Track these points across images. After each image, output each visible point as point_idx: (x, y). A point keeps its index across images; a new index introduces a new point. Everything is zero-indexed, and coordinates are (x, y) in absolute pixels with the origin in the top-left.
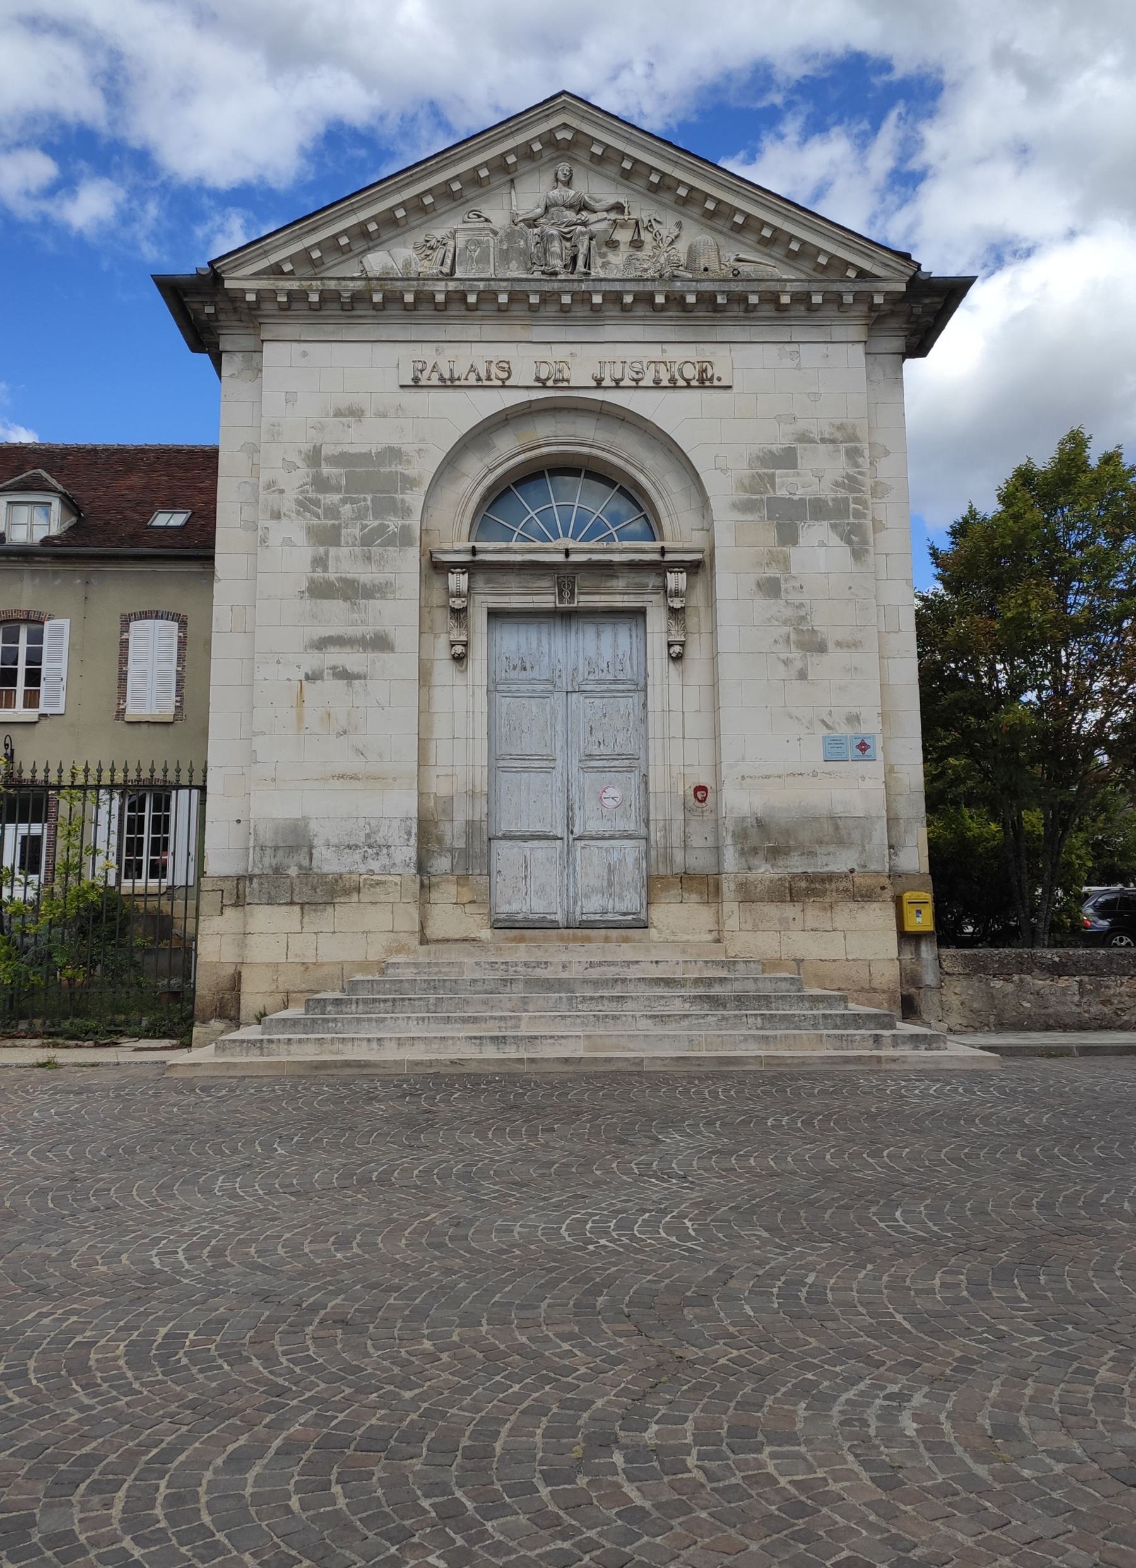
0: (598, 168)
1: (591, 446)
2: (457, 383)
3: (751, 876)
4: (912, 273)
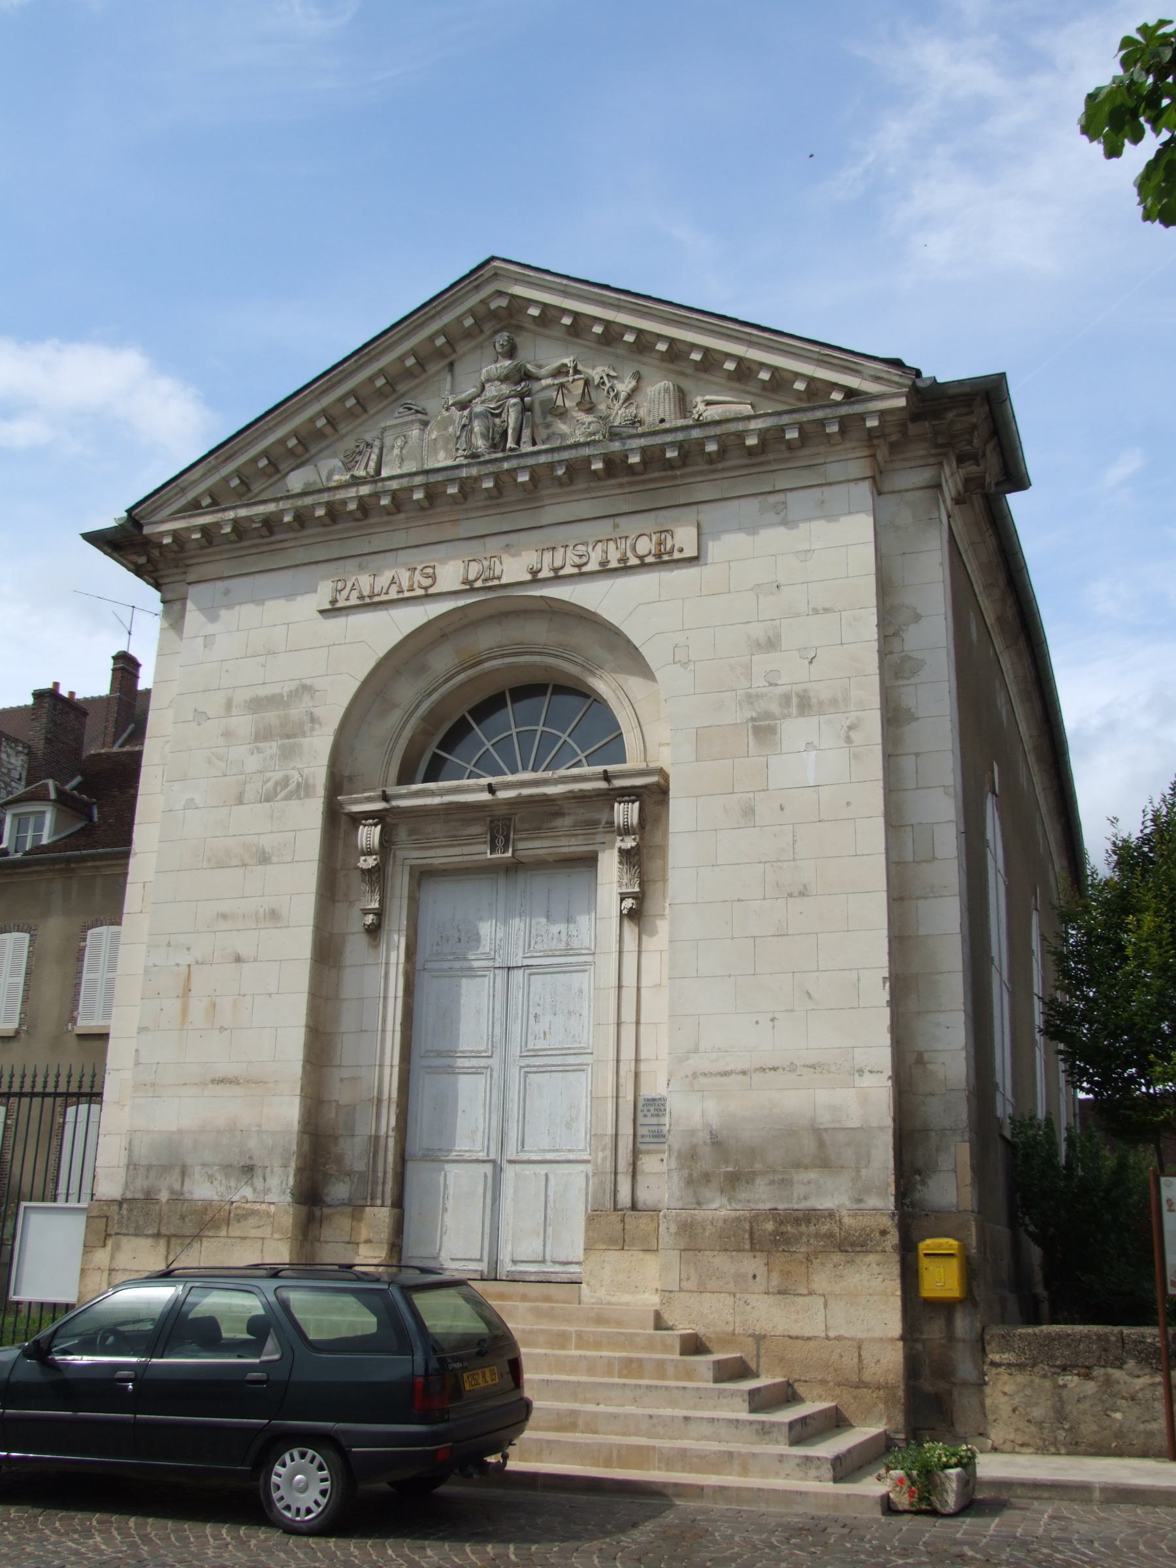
0: (547, 332)
1: (540, 654)
2: (377, 599)
3: (699, 1214)
4: (909, 383)
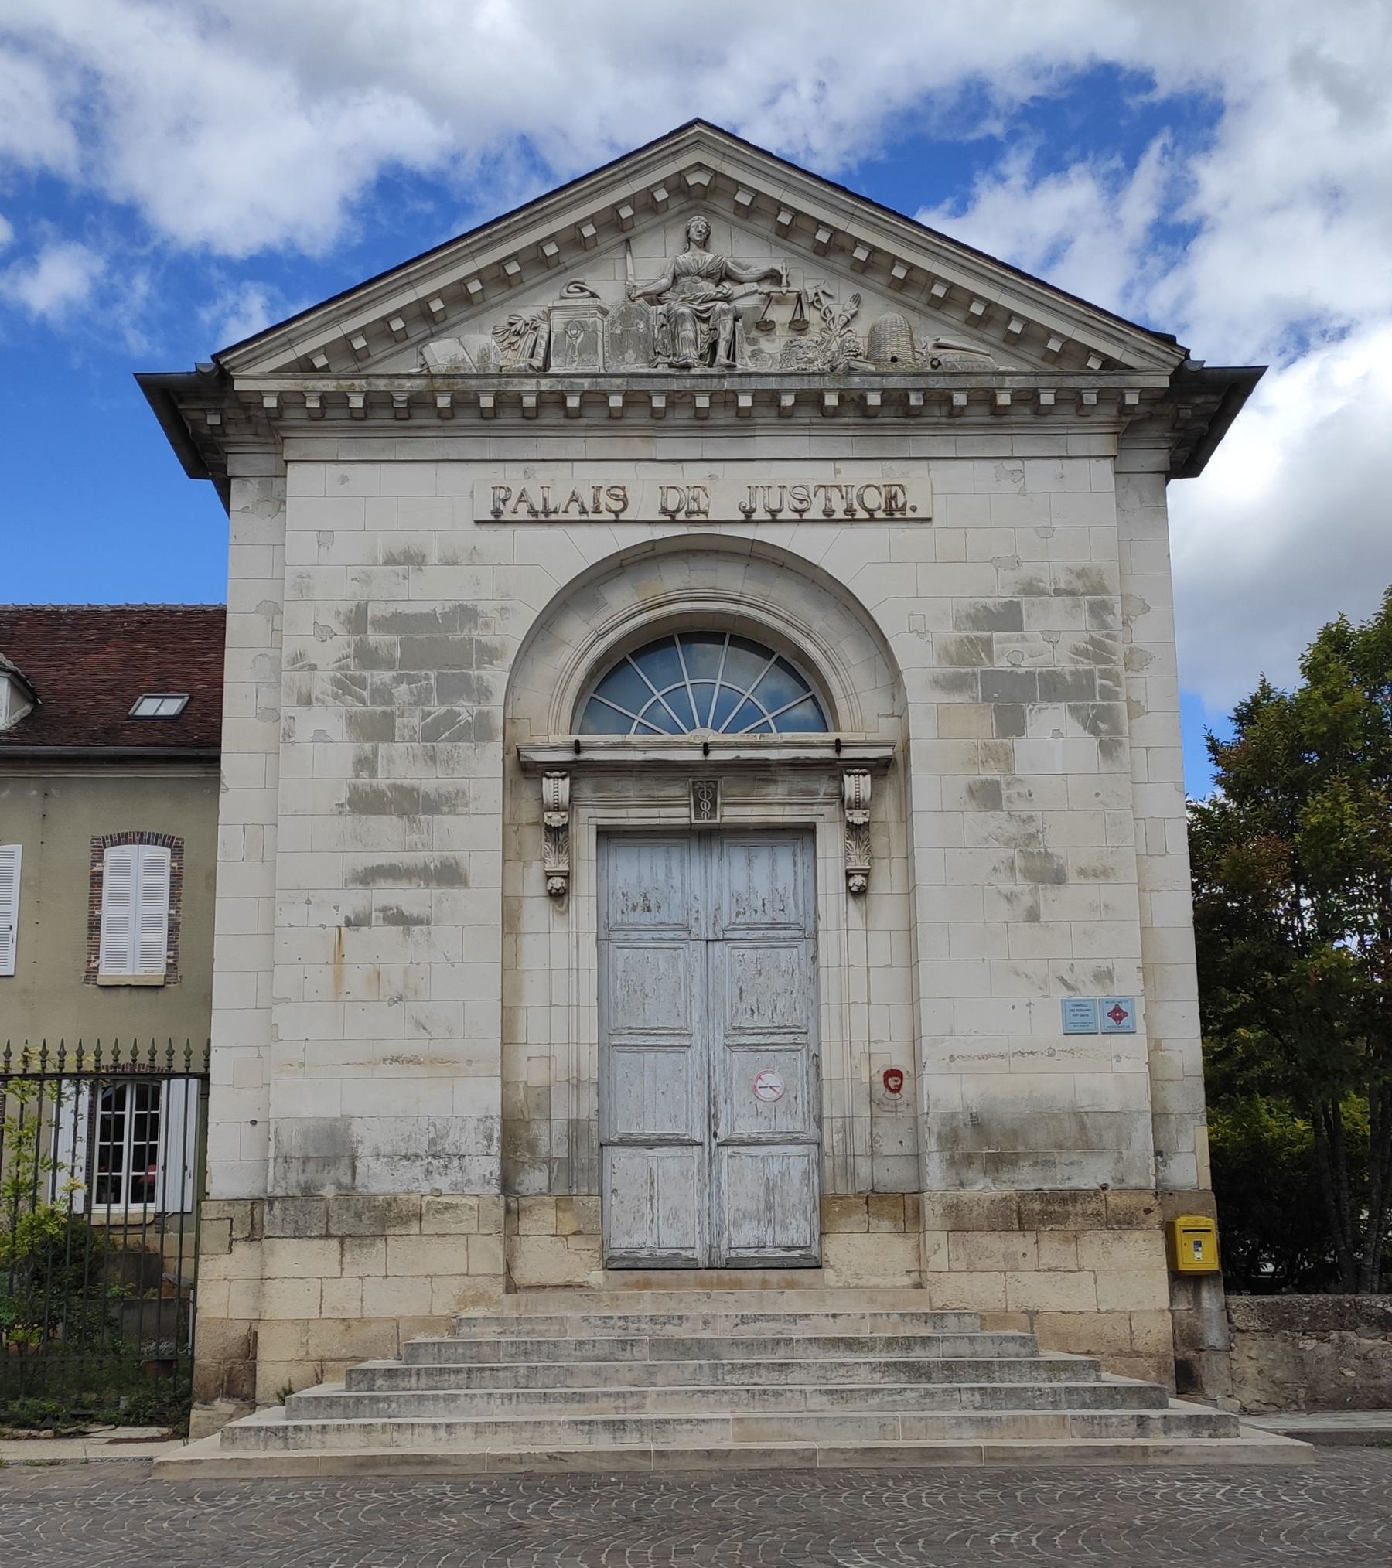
0: (746, 224)
1: (737, 602)
2: (553, 517)
3: (965, 1195)
4: (1177, 363)
